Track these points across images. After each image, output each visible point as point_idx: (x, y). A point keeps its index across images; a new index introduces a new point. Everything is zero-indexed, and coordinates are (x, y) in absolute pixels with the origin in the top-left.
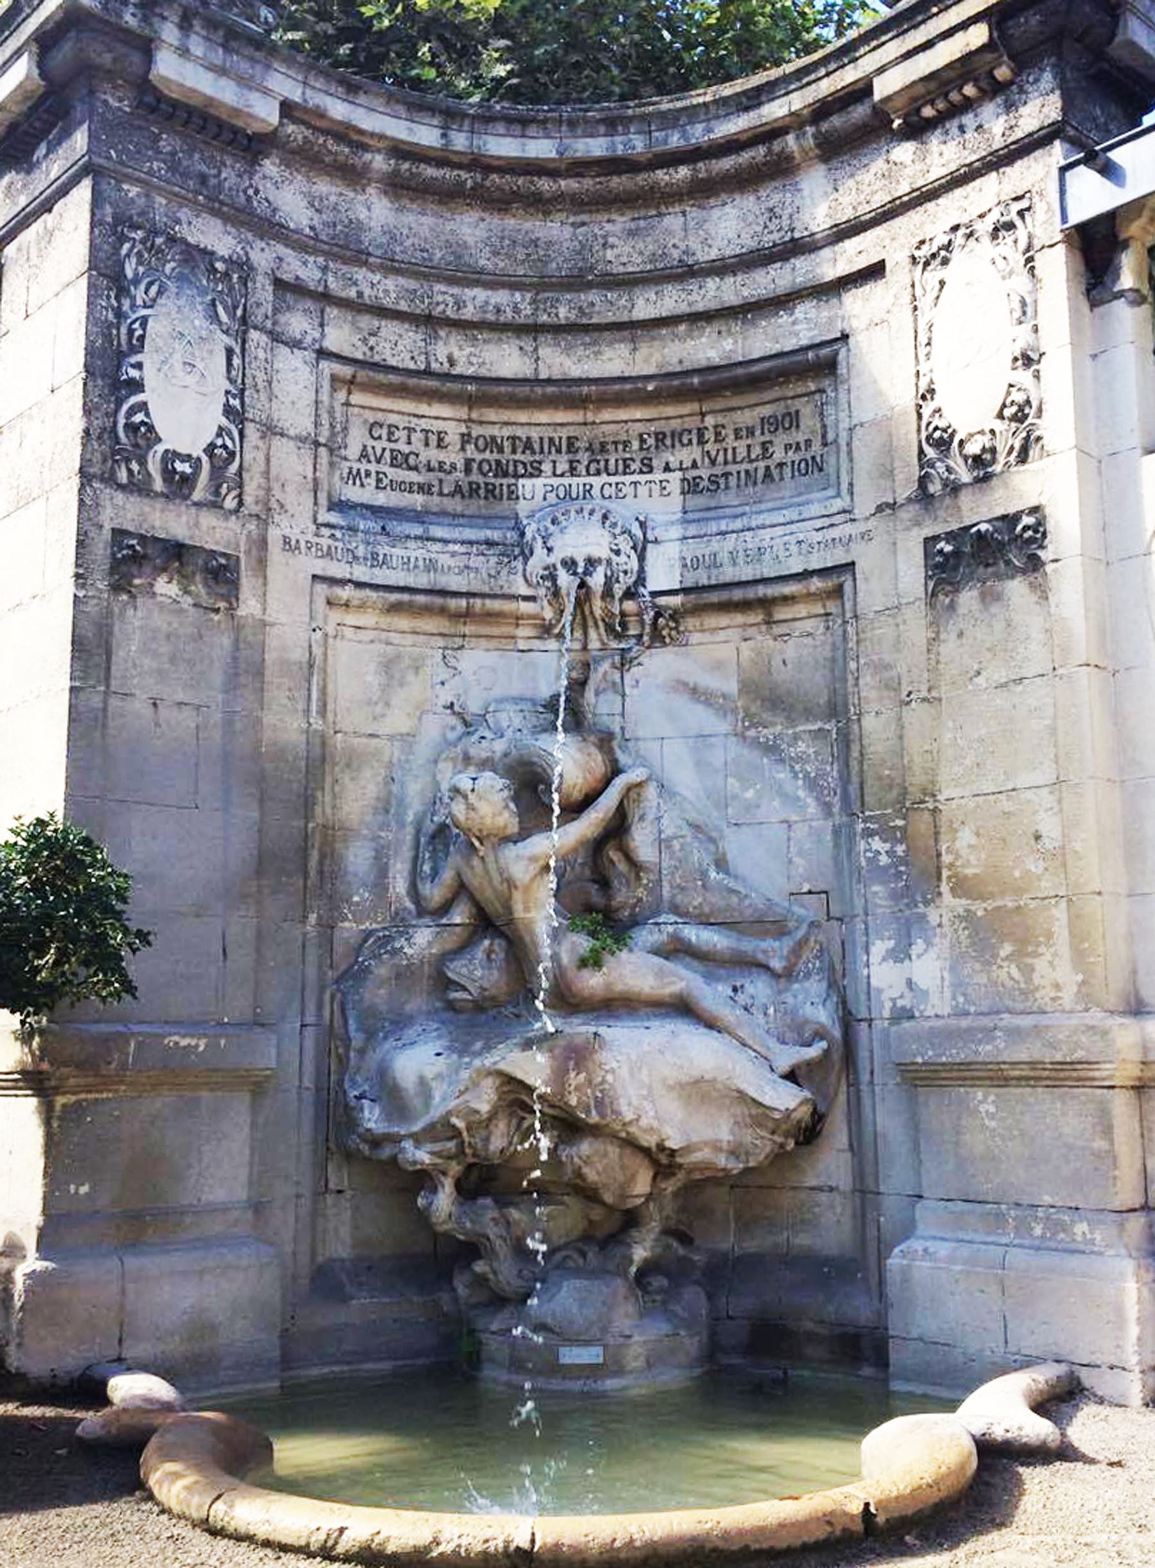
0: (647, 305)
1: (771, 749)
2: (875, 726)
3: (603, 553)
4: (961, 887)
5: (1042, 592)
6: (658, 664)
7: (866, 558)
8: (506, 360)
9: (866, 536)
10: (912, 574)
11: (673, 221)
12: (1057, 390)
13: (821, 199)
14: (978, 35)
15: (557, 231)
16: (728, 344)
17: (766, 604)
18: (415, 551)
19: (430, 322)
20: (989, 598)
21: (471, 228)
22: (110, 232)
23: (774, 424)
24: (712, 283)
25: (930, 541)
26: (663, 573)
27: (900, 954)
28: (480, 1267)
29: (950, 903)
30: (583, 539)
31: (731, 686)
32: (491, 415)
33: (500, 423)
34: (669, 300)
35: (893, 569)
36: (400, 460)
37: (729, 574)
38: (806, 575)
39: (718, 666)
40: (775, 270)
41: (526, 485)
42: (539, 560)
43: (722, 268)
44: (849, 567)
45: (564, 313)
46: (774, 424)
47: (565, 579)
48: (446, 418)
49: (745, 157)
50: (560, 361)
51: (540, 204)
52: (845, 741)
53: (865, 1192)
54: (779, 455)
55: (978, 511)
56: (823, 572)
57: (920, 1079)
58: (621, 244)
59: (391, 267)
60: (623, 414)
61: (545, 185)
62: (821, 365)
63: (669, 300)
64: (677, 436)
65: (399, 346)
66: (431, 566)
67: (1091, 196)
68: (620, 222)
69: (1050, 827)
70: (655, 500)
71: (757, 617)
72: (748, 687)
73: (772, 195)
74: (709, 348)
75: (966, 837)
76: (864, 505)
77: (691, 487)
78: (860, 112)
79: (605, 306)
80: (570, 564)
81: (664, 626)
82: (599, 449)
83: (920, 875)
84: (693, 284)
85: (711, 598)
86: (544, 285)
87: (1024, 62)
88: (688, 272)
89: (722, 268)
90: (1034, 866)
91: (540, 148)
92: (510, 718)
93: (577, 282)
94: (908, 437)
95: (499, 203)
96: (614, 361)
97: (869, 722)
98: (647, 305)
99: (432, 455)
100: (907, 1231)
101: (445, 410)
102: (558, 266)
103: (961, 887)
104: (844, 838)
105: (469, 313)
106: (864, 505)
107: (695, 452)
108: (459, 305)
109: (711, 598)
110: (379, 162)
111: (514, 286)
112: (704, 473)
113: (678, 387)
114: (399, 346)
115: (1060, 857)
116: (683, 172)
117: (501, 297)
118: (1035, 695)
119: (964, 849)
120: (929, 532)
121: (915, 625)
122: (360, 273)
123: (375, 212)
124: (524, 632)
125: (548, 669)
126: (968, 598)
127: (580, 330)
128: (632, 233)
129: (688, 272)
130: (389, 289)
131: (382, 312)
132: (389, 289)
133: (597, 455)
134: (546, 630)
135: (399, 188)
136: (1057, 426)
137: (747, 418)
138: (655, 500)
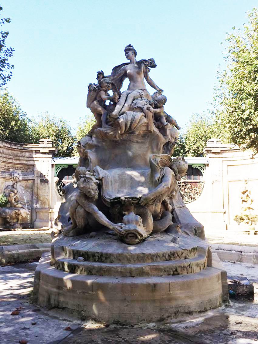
0: (21, 158)
1: (27, 190)
2: (35, 190)
3: (17, 176)
5: (48, 184)
6: (19, 184)
7: (35, 179)
8: (11, 161)
9: (36, 178)
10: (39, 181)
11: (23, 153)
13: (35, 155)
14: (48, 151)
15: (15, 152)
16: (26, 162)
17: (28, 181)
18: (5, 175)
21: (10, 151)
23: (29, 168)
24: (26, 158)
25: (41, 180)
26: (21, 177)
27: (37, 204)
28: (10, 224)
31: (24, 186)
32: (9, 164)
34: (23, 159)
36: (3, 168)
37: (25, 178)
38: (31, 179)
39: (23, 184)
40: (30, 158)
41: (11, 170)
42: (12, 176)
44: (34, 180)
45: (15, 158)
46: (29, 168)
47: (15, 178)
48: (6, 164)
49: (30, 151)
50: (14, 161)
51: (15, 150)
52: (33, 191)
54: (29, 170)
56: (32, 180)
59: (5, 154)
60: (18, 165)
61: (16, 150)
63: (23, 159)
64: (21, 167)
65: (5, 160)
66: (6, 176)
67: (53, 163)
68: (20, 152)
70: (19, 172)
71: (27, 181)
72: (25, 186)
74: (25, 162)
75: (42, 198)
76: (36, 176)
77: (22, 171)
78: (39, 151)
79: (18, 158)
80: (15, 177)
83: (38, 200)
84: (24, 158)
86: (14, 156)
88: (24, 157)
90: (46, 200)
91: (16, 147)
92: (10, 187)
96: (18, 162)
97: (35, 190)
98: (21, 158)
99: (5, 167)
100: (35, 221)
101: (6, 164)
103: (41, 201)
104: (32, 197)
105: (9, 158)
106: (36, 176)
107: (22, 169)
108: (8, 157)
109: (23, 179)
110: (6, 148)
112: (23, 170)
113: (22, 164)
115: (48, 200)
116: (25, 151)
117: (11, 156)
118: (47, 190)
119: (41, 199)
120: (41, 179)
121: (39, 184)
122: (4, 155)
123: (5, 150)
124: (10, 180)
125: (11, 184)
127: (16, 159)
128: (20, 153)
129: (24, 157)
130: (4, 156)
131: (4, 157)
132: (4, 156)
134: (12, 181)
135: (7, 149)
137: (26, 167)
138: (19, 172)
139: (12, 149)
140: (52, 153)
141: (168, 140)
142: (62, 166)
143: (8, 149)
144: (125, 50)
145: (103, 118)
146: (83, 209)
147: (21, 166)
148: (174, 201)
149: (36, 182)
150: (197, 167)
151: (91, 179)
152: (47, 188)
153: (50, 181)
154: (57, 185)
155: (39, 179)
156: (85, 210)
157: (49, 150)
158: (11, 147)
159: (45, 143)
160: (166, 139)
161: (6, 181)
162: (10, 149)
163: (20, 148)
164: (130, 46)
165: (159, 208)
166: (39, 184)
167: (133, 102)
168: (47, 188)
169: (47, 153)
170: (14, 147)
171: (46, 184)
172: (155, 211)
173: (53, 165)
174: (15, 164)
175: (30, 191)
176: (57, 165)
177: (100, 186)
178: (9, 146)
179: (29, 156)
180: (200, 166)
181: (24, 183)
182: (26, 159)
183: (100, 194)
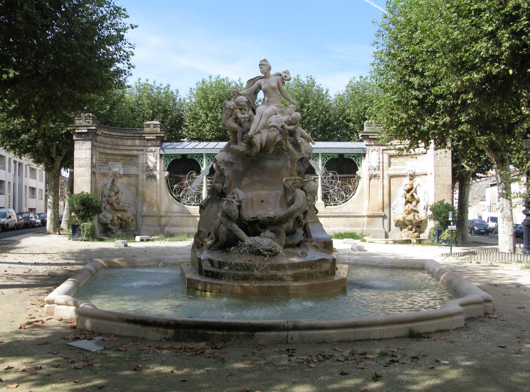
0: (121, 148)
2: (140, 189)
4: (148, 202)
7: (140, 174)
8: (109, 151)
10: (145, 177)
11: (124, 141)
12: (158, 165)
14: (155, 137)
15: (114, 140)
19: (104, 148)
20: (151, 180)
21: (108, 139)
22: (93, 145)
23: (131, 160)
29: (146, 203)
30: (116, 170)
33: (108, 157)
34: (123, 148)
35: (143, 176)
36: (101, 160)
43: (128, 146)
46: (131, 160)
48: (104, 156)
50: (114, 152)
51: (114, 138)
52: (137, 189)
53: (137, 225)
55: (151, 174)
57: (143, 216)
58: (120, 142)
59: (103, 143)
62: (137, 156)
63: (123, 148)
65: (102, 150)
67: (162, 152)
68: (119, 140)
69: (155, 199)
73: (133, 141)
77: (123, 164)
81: (121, 177)
82: (115, 160)
83: (144, 201)
85: (125, 175)
86: (113, 145)
87: (157, 139)
88: (125, 146)
89: (128, 146)
91: (115, 134)
93: (116, 145)
94: (145, 166)
95: (110, 137)
98: (121, 148)
102: (114, 143)
109: (125, 175)
111: (110, 145)
113: (123, 155)
114: (102, 150)
121: (145, 181)
126: (149, 180)
127: (116, 149)
130: (102, 145)
132: (102, 145)
133: (115, 160)
136: (158, 168)
138: (120, 165)
139: (110, 136)
140: (160, 139)
141: (302, 156)
142: (173, 156)
143: (106, 136)
144: (260, 65)
145: (239, 135)
146: (225, 227)
147: (122, 158)
148: (307, 217)
149: (140, 177)
150: (351, 158)
151: (233, 202)
152: (155, 185)
153: (158, 177)
154: (167, 182)
155: (145, 174)
156: (227, 228)
157: (157, 136)
158: (110, 133)
159: (152, 126)
160: (300, 155)
161: (104, 177)
162: (108, 137)
163: (119, 134)
164: (265, 60)
165: (291, 224)
166: (145, 181)
167: (267, 120)
168: (155, 185)
169: (154, 140)
170: (113, 134)
171: (153, 180)
172: (288, 228)
173: (161, 155)
174: (114, 155)
175: (133, 189)
176: (167, 156)
177: (239, 207)
178: (108, 133)
179: (131, 144)
180: (354, 156)
181: (125, 180)
182: (127, 148)
183: (239, 214)
